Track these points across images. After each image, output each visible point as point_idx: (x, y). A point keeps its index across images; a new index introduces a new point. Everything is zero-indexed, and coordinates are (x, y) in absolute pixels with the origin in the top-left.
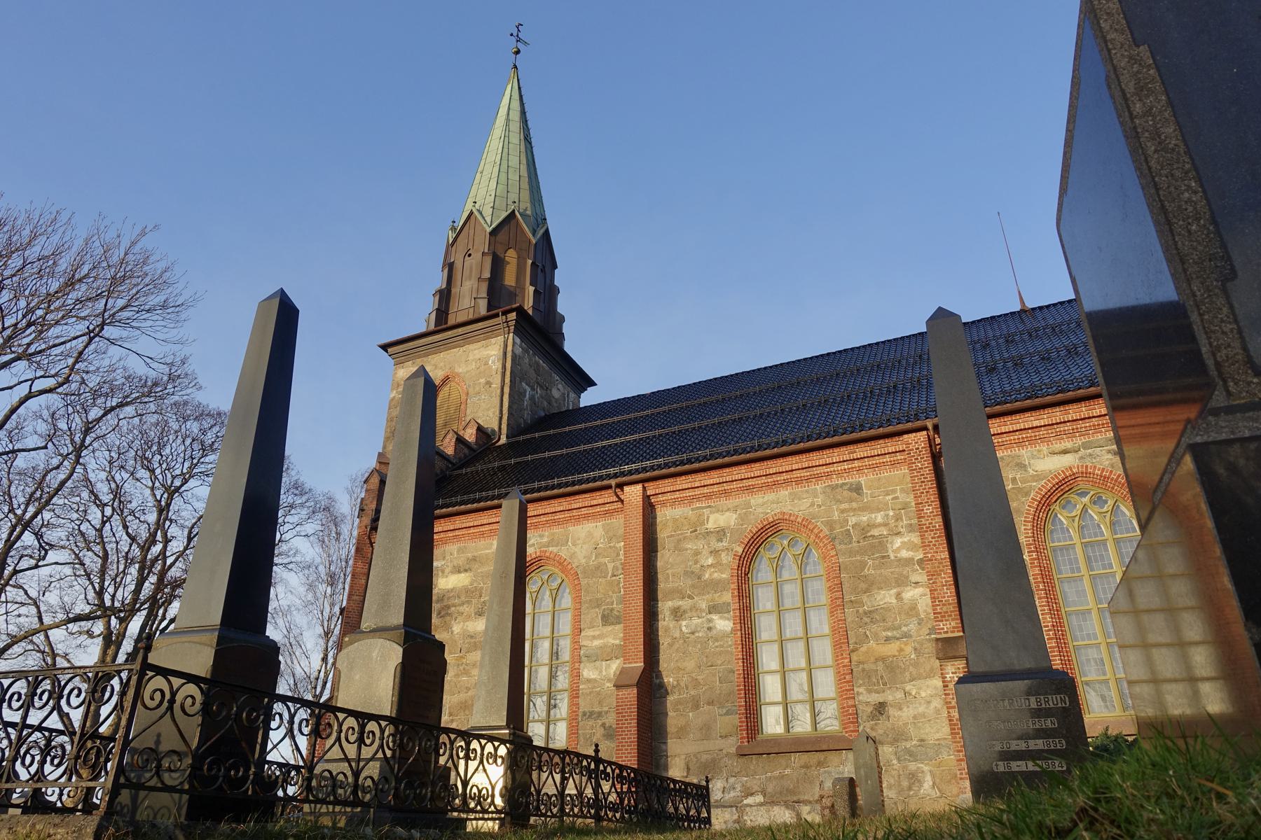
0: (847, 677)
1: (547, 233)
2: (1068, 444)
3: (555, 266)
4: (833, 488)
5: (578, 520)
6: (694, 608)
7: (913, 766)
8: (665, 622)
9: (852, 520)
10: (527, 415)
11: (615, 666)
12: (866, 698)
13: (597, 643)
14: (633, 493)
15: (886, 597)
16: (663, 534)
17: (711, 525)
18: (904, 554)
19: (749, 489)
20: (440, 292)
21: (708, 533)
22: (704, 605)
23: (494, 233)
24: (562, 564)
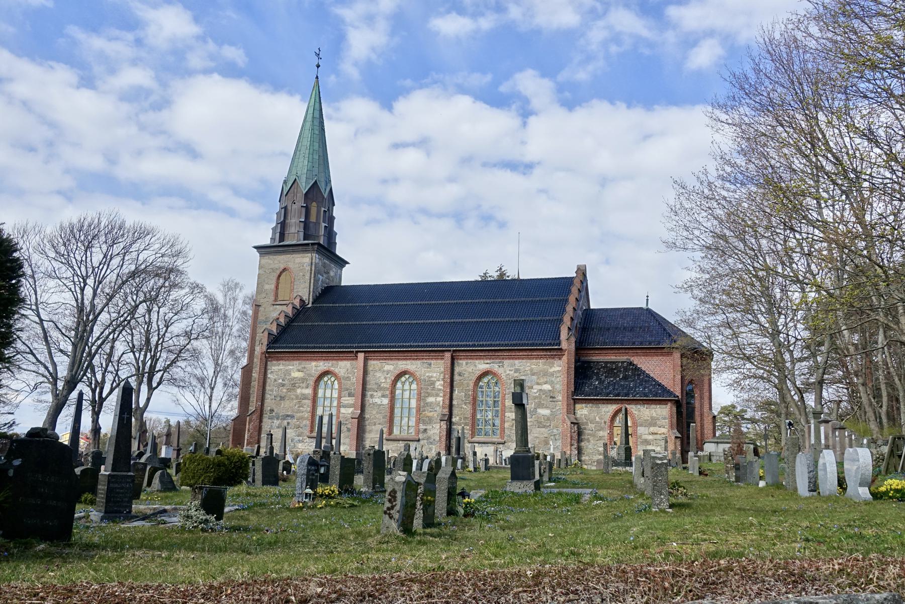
0: (418, 422)
1: (331, 189)
2: (488, 361)
3: (334, 205)
5: (342, 360)
7: (431, 446)
9: (427, 374)
11: (351, 410)
12: (422, 427)
15: (431, 399)
19: (398, 359)
21: (384, 371)
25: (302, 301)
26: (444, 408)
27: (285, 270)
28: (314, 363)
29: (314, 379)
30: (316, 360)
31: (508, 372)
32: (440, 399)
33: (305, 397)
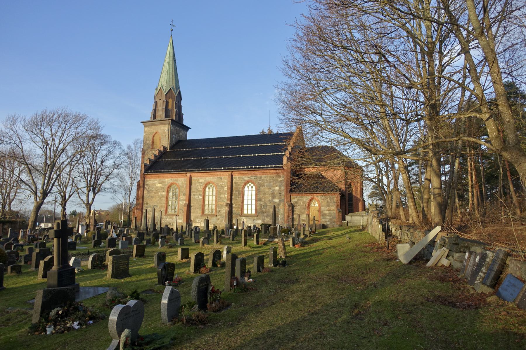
0: (216, 206)
1: (180, 93)
3: (181, 100)
6: (197, 194)
8: (192, 196)
10: (174, 142)
11: (185, 202)
12: (218, 210)
14: (188, 175)
15: (223, 196)
16: (193, 182)
17: (200, 181)
18: (226, 190)
20: (154, 110)
23: (166, 95)
24: (177, 184)
25: (165, 148)
26: (228, 200)
27: (156, 133)
28: (166, 180)
29: (167, 187)
30: (167, 178)
31: (259, 181)
32: (226, 196)
33: (163, 196)
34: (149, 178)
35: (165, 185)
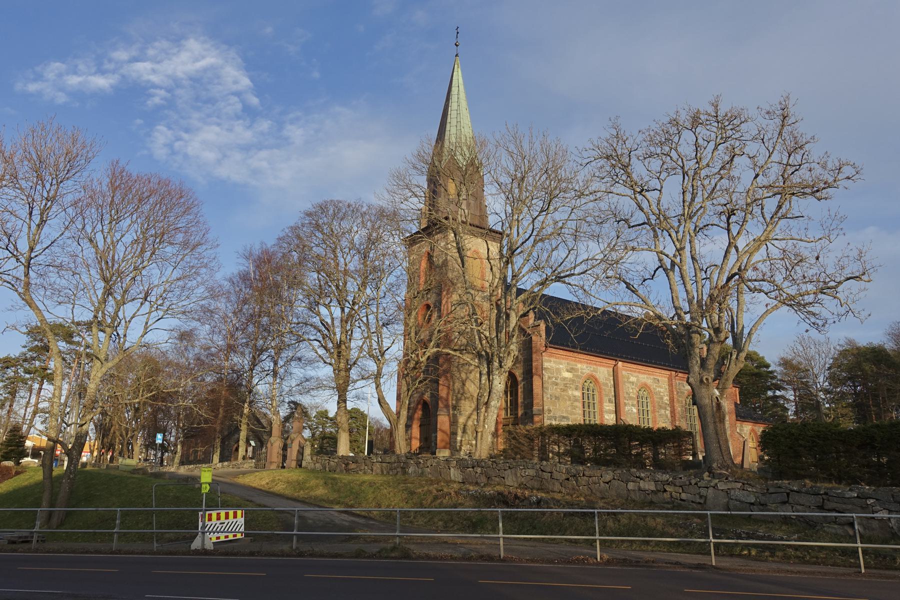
4: (655, 379)
5: (601, 365)
6: (629, 404)
13: (608, 408)
18: (666, 402)
19: (639, 372)
22: (631, 403)
28: (579, 366)
34: (551, 356)
35: (577, 376)
